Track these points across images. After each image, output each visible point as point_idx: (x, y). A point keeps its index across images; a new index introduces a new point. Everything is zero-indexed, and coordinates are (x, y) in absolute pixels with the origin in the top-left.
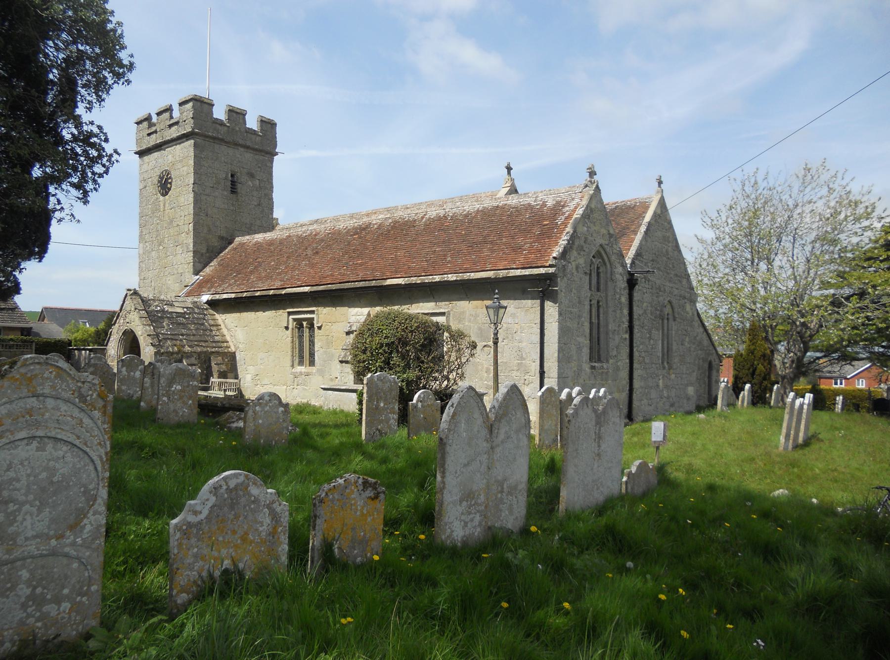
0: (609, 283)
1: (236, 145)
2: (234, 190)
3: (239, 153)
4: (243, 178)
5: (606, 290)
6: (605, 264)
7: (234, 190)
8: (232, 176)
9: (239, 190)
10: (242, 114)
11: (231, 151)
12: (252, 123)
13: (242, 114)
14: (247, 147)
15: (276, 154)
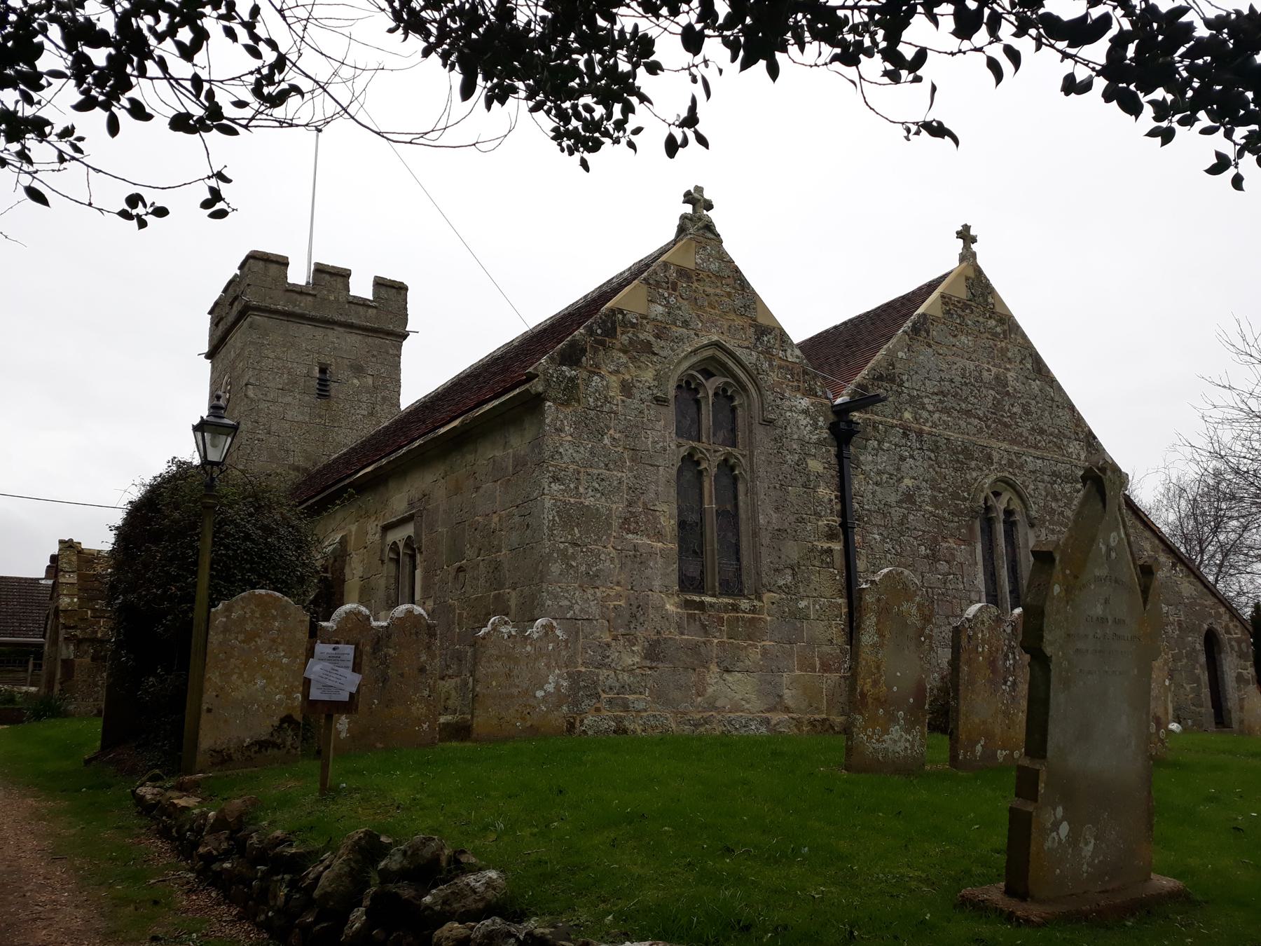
0: (760, 433)
1: (329, 323)
2: (323, 388)
3: (335, 337)
4: (340, 372)
5: (750, 444)
6: (744, 388)
7: (323, 388)
8: (323, 371)
9: (333, 393)
10: (344, 275)
11: (319, 333)
12: (361, 288)
13: (344, 275)
14: (351, 326)
15: (405, 336)
